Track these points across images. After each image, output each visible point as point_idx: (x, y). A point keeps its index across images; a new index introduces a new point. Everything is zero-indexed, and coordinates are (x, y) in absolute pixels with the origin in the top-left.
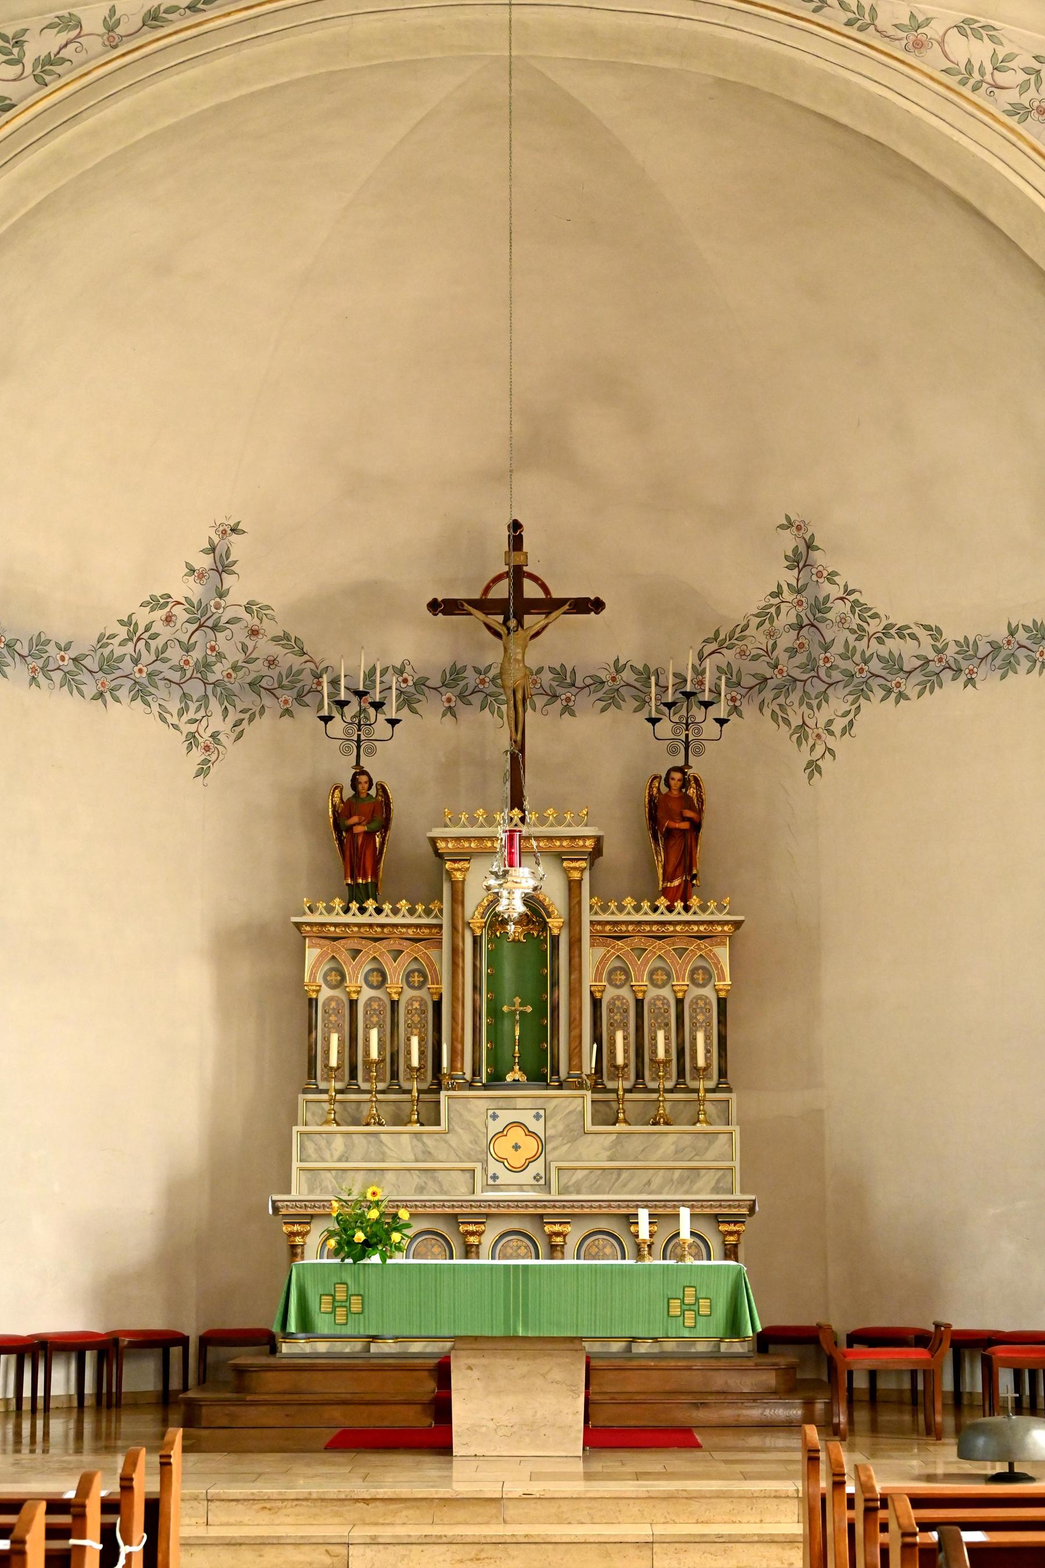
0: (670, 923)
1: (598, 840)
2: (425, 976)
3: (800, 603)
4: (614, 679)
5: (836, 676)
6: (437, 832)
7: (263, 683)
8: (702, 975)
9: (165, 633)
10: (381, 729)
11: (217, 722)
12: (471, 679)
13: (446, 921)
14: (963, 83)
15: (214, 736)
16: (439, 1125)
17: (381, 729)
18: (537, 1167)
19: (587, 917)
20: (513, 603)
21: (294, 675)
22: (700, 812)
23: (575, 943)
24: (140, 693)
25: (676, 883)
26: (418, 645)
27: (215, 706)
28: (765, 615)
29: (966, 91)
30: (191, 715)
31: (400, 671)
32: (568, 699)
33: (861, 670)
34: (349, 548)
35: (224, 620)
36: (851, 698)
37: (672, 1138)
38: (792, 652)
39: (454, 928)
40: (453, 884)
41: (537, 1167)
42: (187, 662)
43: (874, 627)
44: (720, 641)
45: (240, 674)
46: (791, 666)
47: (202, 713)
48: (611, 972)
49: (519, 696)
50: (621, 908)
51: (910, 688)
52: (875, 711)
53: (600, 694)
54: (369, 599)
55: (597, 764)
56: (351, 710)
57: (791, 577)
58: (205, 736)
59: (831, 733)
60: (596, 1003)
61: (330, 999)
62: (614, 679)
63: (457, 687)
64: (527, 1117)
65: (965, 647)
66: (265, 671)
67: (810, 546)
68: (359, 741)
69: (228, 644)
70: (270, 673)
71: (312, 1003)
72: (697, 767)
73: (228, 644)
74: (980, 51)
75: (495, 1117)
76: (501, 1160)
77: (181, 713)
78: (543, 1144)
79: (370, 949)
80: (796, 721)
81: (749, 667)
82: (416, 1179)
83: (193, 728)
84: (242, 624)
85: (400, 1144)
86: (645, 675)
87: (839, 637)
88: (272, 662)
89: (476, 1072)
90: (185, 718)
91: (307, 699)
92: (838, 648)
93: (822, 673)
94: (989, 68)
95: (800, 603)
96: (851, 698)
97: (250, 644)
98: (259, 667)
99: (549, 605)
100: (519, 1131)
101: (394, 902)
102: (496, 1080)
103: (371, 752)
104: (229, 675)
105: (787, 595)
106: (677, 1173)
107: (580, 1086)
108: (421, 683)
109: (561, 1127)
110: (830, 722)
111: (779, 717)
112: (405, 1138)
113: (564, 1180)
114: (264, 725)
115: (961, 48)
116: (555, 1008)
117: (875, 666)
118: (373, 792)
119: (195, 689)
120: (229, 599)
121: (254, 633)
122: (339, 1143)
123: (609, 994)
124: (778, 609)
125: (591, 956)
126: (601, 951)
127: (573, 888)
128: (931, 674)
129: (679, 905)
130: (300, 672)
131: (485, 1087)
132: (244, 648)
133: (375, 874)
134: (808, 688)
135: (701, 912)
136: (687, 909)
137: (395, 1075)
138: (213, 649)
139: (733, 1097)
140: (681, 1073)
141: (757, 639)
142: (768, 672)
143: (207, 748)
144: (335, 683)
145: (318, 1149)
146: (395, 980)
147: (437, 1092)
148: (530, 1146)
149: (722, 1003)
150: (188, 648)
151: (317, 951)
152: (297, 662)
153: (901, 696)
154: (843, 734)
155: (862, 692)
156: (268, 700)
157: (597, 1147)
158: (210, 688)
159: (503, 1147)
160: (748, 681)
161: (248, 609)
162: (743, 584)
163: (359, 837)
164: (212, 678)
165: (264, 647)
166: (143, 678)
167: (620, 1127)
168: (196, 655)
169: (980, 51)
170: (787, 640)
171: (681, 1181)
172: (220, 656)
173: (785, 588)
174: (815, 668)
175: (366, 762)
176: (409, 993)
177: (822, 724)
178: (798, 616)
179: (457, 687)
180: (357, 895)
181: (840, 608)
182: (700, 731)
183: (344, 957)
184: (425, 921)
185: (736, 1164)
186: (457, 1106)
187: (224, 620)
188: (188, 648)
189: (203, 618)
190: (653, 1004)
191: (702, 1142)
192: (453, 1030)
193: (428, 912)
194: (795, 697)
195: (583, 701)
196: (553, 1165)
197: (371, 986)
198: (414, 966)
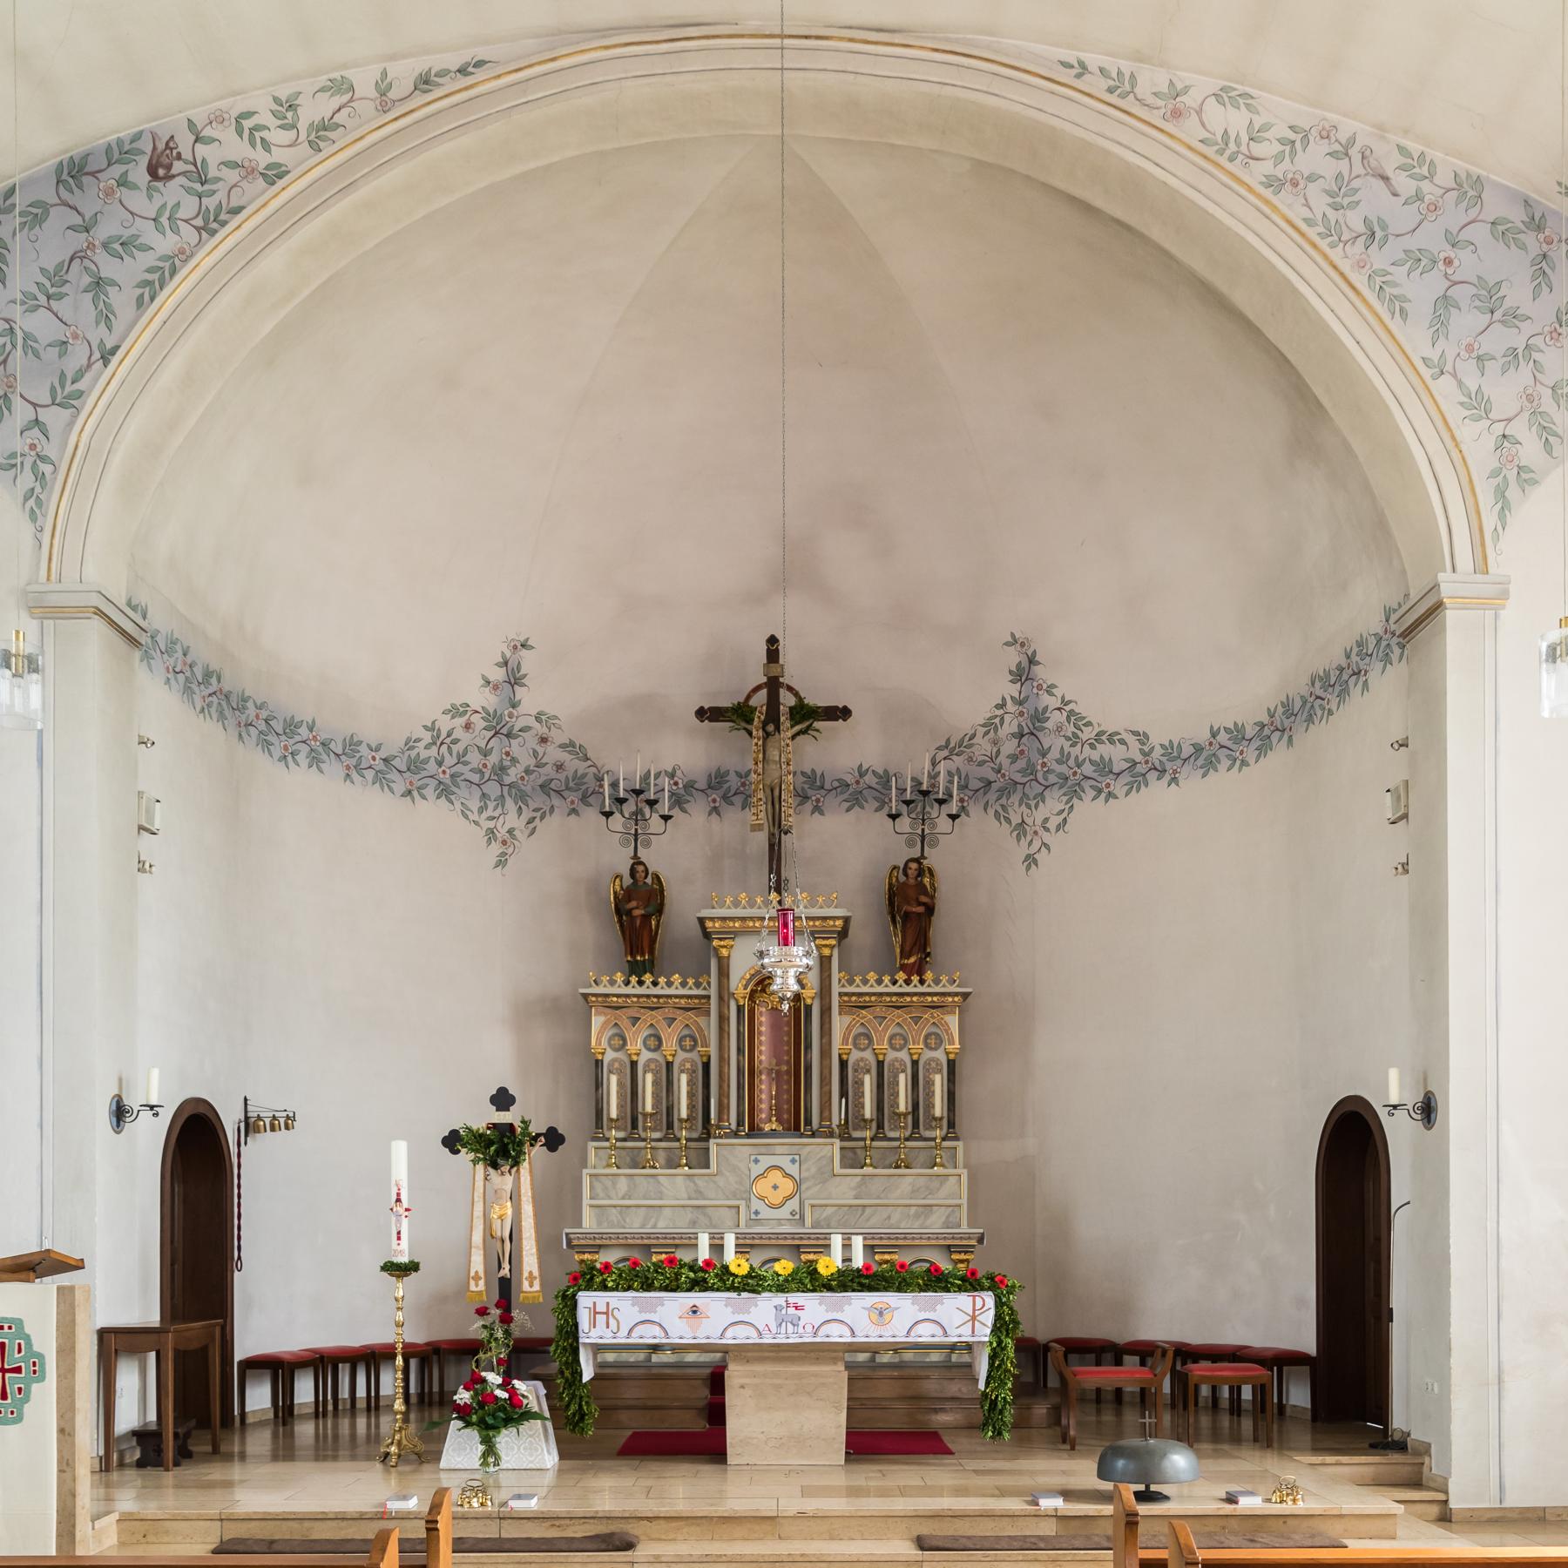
0: (908, 994)
1: (847, 920)
2: (695, 1040)
3: (1021, 714)
4: (858, 782)
5: (1052, 778)
6: (705, 913)
7: (552, 785)
8: (934, 1040)
10: (655, 823)
11: (512, 819)
12: (734, 782)
13: (713, 992)
14: (1221, 152)
15: (510, 832)
16: (708, 1167)
17: (655, 823)
18: (793, 1204)
19: (836, 989)
21: (579, 779)
22: (933, 897)
23: (826, 1012)
24: (445, 792)
25: (912, 960)
26: (688, 751)
27: (509, 803)
28: (990, 725)
29: (1223, 161)
30: (490, 812)
31: (672, 775)
32: (818, 800)
33: (1075, 774)
34: (631, 669)
35: (517, 728)
36: (1065, 799)
37: (910, 1179)
38: (1014, 758)
39: (721, 998)
40: (720, 959)
41: (793, 1204)
42: (485, 766)
43: (1087, 734)
44: (951, 748)
45: (532, 777)
46: (1013, 771)
47: (499, 810)
48: (855, 1038)
49: (776, 793)
50: (865, 982)
51: (1118, 787)
52: (1088, 809)
53: (846, 796)
54: (643, 711)
55: (845, 854)
56: (629, 808)
57: (1013, 690)
58: (502, 833)
59: (1047, 830)
60: (843, 1064)
61: (614, 1060)
62: (858, 782)
63: (720, 789)
64: (784, 1161)
66: (553, 774)
68: (636, 835)
69: (522, 750)
70: (558, 776)
71: (598, 1064)
72: (933, 859)
74: (1236, 121)
75: (756, 1161)
76: (762, 1199)
77: (481, 810)
78: (798, 1184)
79: (648, 1017)
80: (1016, 820)
81: (976, 772)
82: (689, 1215)
83: (491, 824)
84: (533, 732)
85: (675, 1185)
86: (885, 779)
88: (559, 767)
89: (740, 1123)
90: (485, 815)
91: (590, 800)
92: (1054, 754)
93: (1040, 776)
94: (1245, 138)
95: (1021, 714)
96: (1065, 799)
97: (540, 750)
98: (549, 771)
99: (806, 715)
100: (778, 1173)
101: (668, 977)
102: (754, 1131)
103: (648, 844)
104: (522, 778)
105: (1010, 707)
106: (913, 1210)
107: (831, 1135)
108: (690, 786)
109: (813, 1170)
110: (1046, 820)
112: (680, 1180)
113: (816, 1216)
114: (555, 822)
115: (1222, 118)
116: (808, 1068)
117: (1088, 769)
118: (649, 880)
119: (493, 789)
120: (521, 709)
121: (544, 740)
122: (623, 1184)
123: (855, 1055)
124: (1002, 719)
125: (839, 1023)
126: (847, 1019)
127: (824, 962)
128: (1136, 774)
129: (915, 979)
130: (584, 775)
131: (748, 1136)
132: (535, 752)
133: (652, 952)
134: (1027, 789)
135: (934, 984)
136: (922, 982)
137: (670, 1126)
138: (507, 754)
139: (960, 1144)
140: (916, 1125)
141: (983, 747)
142: (992, 776)
143: (504, 843)
144: (614, 785)
145: (605, 1189)
146: (670, 1045)
147: (707, 1140)
148: (787, 1186)
149: (952, 1065)
150: (485, 753)
151: (602, 1019)
152: (582, 767)
153: (1110, 795)
154: (1058, 830)
155: (1075, 793)
156: (556, 801)
157: (845, 1187)
158: (506, 789)
159: (762, 1187)
160: (974, 784)
161: (538, 719)
162: (971, 696)
163: (637, 920)
164: (507, 780)
165: (553, 754)
166: (446, 779)
167: (868, 1170)
168: (493, 759)
169: (1236, 121)
170: (1009, 747)
171: (917, 1216)
172: (514, 761)
173: (1009, 701)
174: (1034, 772)
175: (642, 853)
176: (682, 1055)
177: (1039, 821)
178: (1020, 725)
179: (720, 789)
180: (635, 970)
181: (1056, 718)
182: (934, 826)
183: (625, 1023)
184: (695, 992)
185: (964, 1201)
186: (725, 1152)
187: (517, 728)
188: (485, 753)
189: (499, 728)
190: (892, 1065)
191: (935, 1183)
192: (720, 1087)
193: (698, 985)
194: (1015, 798)
195: (831, 802)
196: (807, 1203)
197: (649, 1049)
198: (686, 1032)
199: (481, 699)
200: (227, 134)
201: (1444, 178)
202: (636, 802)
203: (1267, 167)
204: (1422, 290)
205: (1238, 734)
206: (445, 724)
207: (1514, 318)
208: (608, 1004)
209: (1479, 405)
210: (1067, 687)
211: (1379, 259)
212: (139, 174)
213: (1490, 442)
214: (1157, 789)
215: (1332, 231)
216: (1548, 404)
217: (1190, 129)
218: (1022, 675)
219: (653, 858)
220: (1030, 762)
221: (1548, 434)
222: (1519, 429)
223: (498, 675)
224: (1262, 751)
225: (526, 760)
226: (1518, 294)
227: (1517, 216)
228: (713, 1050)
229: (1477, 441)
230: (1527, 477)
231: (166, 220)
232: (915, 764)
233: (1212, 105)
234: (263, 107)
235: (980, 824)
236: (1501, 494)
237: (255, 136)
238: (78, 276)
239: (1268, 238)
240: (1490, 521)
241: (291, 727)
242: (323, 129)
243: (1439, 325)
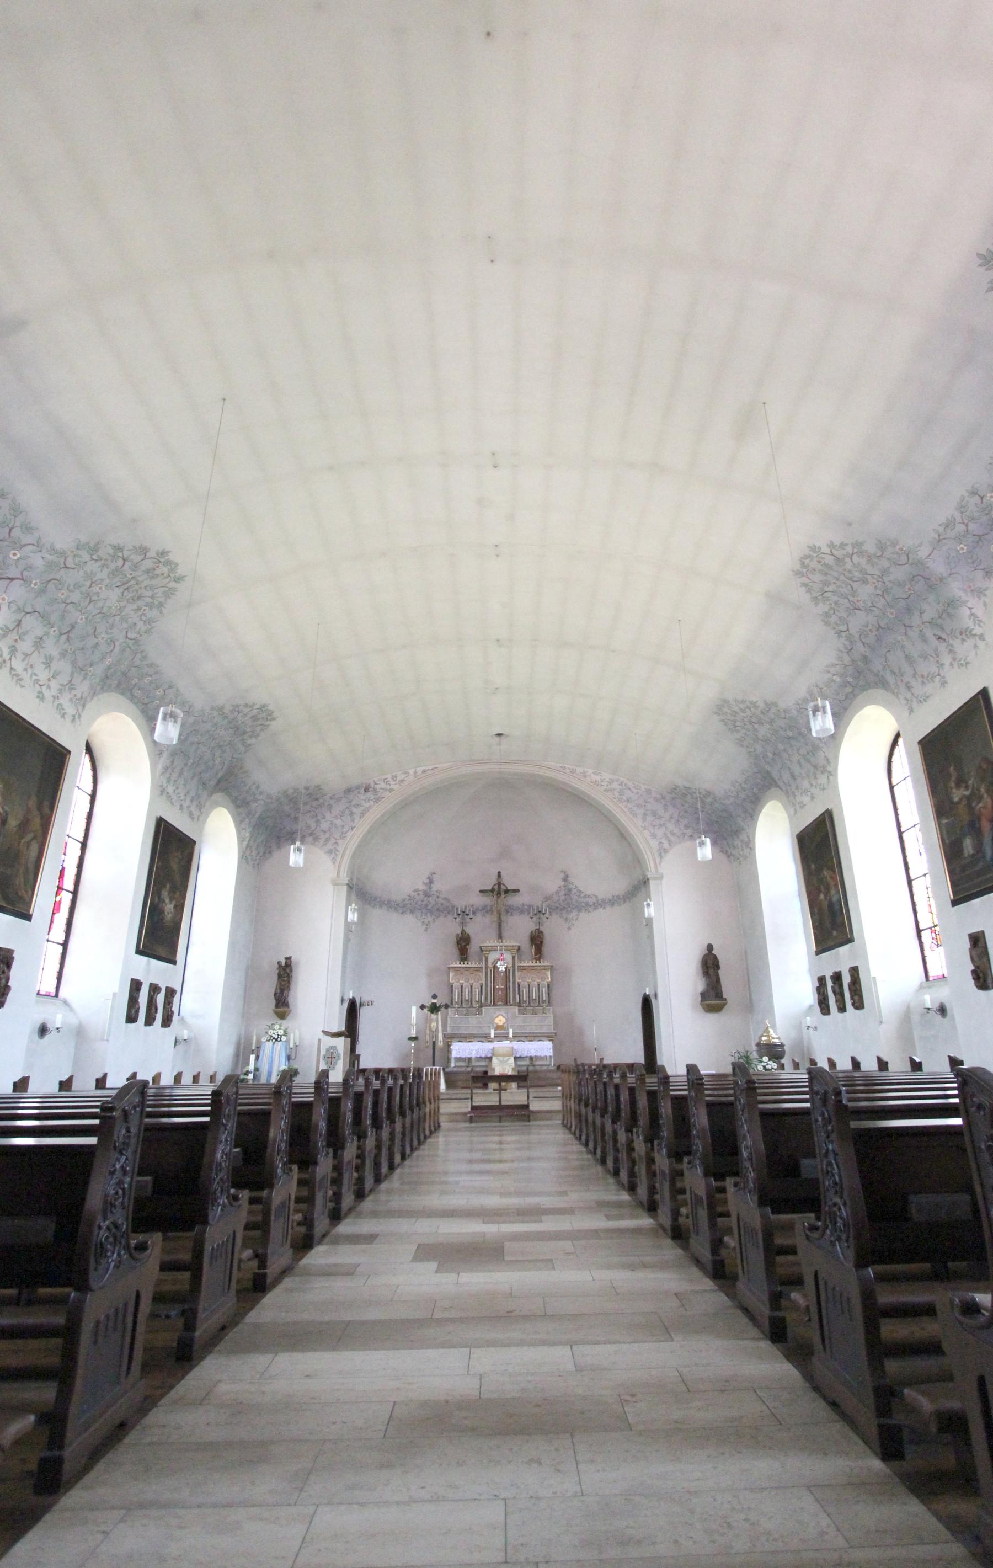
9: (417, 898)
11: (430, 919)
21: (447, 907)
119: (424, 911)
165: (440, 901)
189: (426, 894)
204: (640, 812)
206: (413, 894)
207: (660, 817)
209: (654, 836)
211: (630, 805)
212: (362, 791)
215: (620, 800)
216: (669, 835)
217: (588, 778)
221: (670, 841)
226: (661, 812)
227: (659, 797)
229: (654, 844)
230: (666, 851)
231: (368, 800)
234: (389, 776)
236: (660, 855)
237: (387, 782)
238: (347, 812)
240: (658, 861)
242: (402, 781)
243: (644, 819)
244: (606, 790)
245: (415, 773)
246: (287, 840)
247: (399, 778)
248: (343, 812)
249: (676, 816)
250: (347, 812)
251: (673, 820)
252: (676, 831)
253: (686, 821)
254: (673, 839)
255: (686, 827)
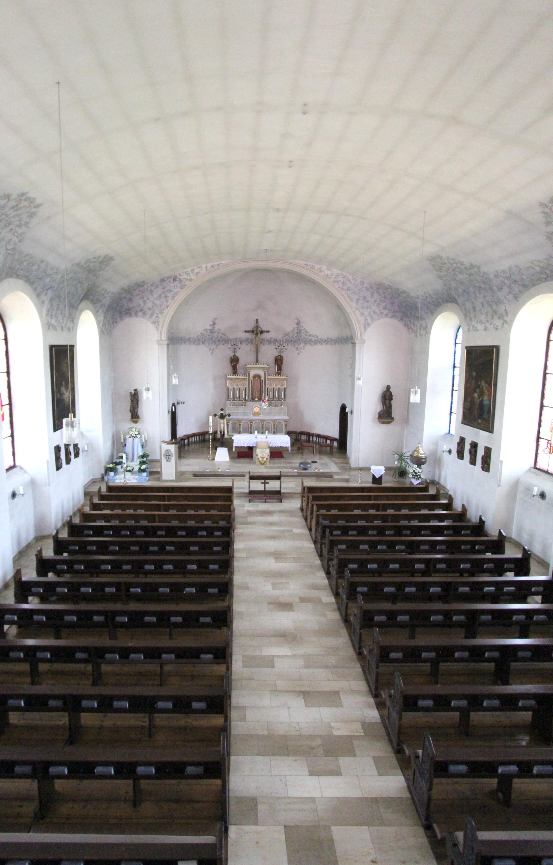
11: (214, 346)
13: (247, 377)
19: (267, 377)
20: (257, 331)
21: (224, 339)
24: (203, 343)
28: (293, 331)
38: (296, 337)
43: (308, 334)
44: (286, 334)
51: (313, 344)
52: (308, 347)
57: (296, 326)
65: (321, 339)
67: (299, 322)
69: (215, 335)
72: (282, 355)
73: (215, 335)
87: (303, 335)
99: (262, 332)
108: (243, 340)
111: (294, 346)
119: (211, 342)
127: (265, 374)
141: (291, 334)
149: (285, 389)
155: (306, 343)
162: (289, 326)
165: (220, 335)
168: (210, 337)
170: (295, 335)
181: (303, 331)
189: (212, 331)
199: (209, 327)
200: (184, 275)
201: (358, 281)
202: (235, 344)
203: (332, 280)
205: (331, 340)
208: (230, 379)
209: (362, 314)
210: (305, 327)
212: (172, 281)
213: (363, 320)
214: (319, 347)
215: (342, 289)
218: (298, 323)
219: (238, 354)
220: (298, 338)
222: (369, 318)
223: (211, 324)
224: (335, 344)
225: (216, 336)
226: (369, 298)
228: (247, 386)
229: (362, 320)
230: (369, 325)
232: (279, 336)
233: (326, 271)
234: (189, 270)
235: (290, 347)
236: (365, 327)
238: (163, 295)
239: (333, 290)
241: (182, 339)
242: (197, 273)
244: (334, 282)
245: (206, 267)
246: (126, 314)
247: (195, 271)
248: (160, 295)
249: (378, 300)
250: (163, 295)
251: (376, 304)
252: (377, 311)
253: (383, 305)
254: (375, 316)
255: (385, 308)
